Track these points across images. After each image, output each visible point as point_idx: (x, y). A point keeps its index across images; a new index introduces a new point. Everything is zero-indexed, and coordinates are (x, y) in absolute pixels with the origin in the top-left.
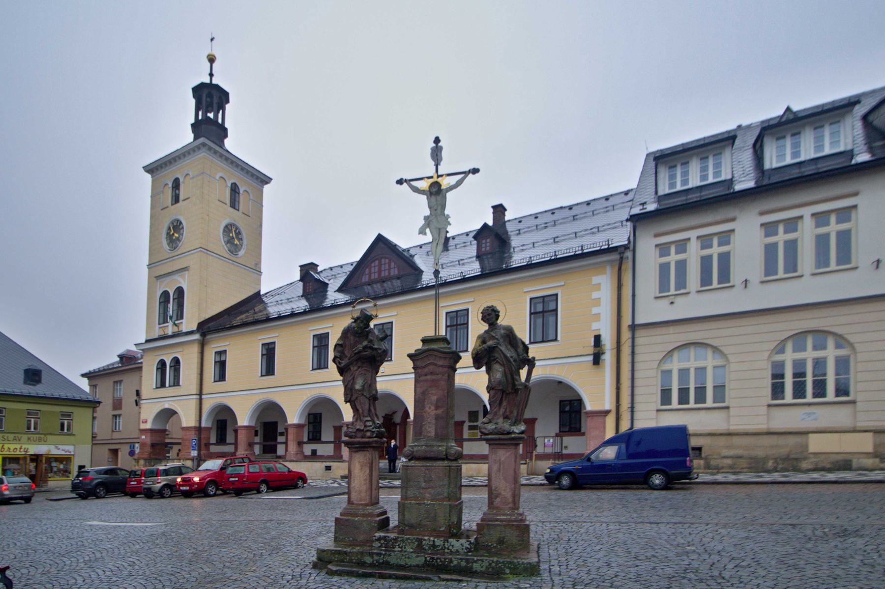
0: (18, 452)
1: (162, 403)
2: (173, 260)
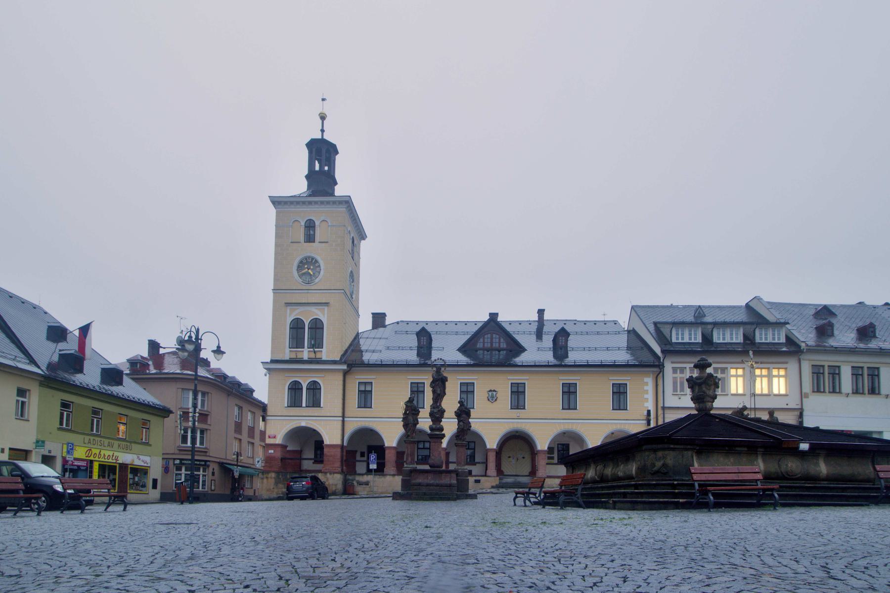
0: (110, 460)
1: (297, 422)
2: (308, 293)
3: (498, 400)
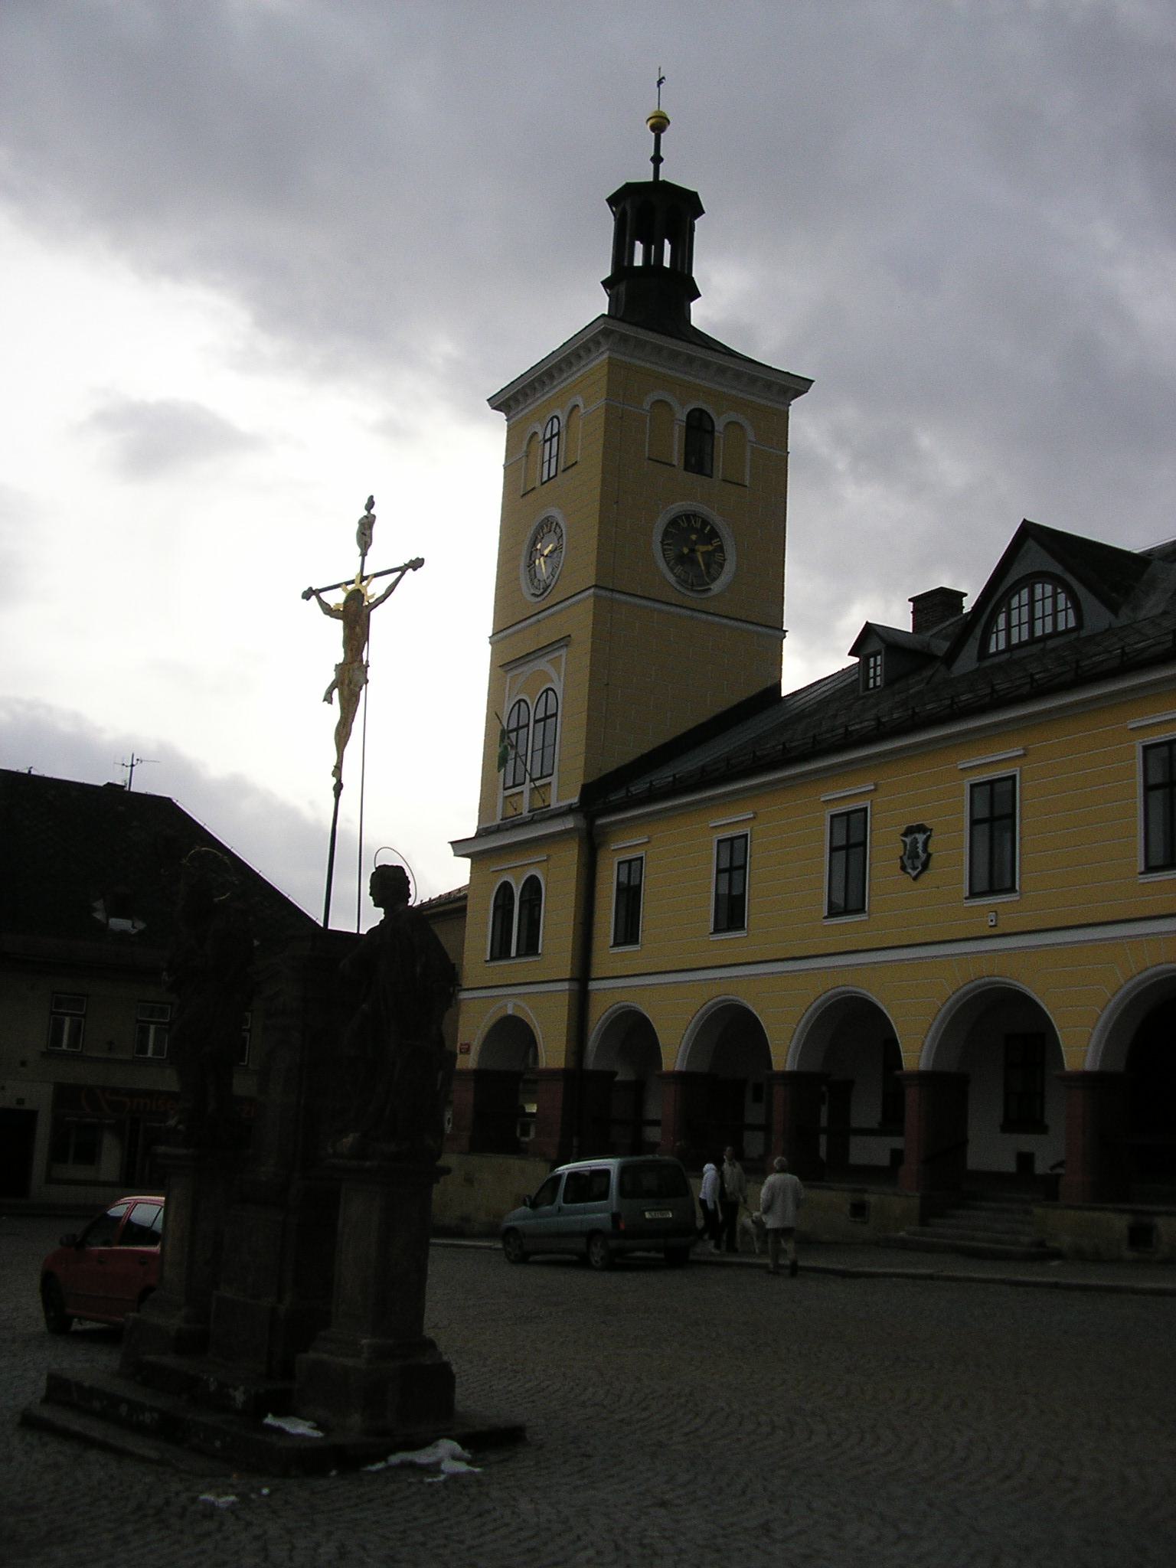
3: (932, 864)
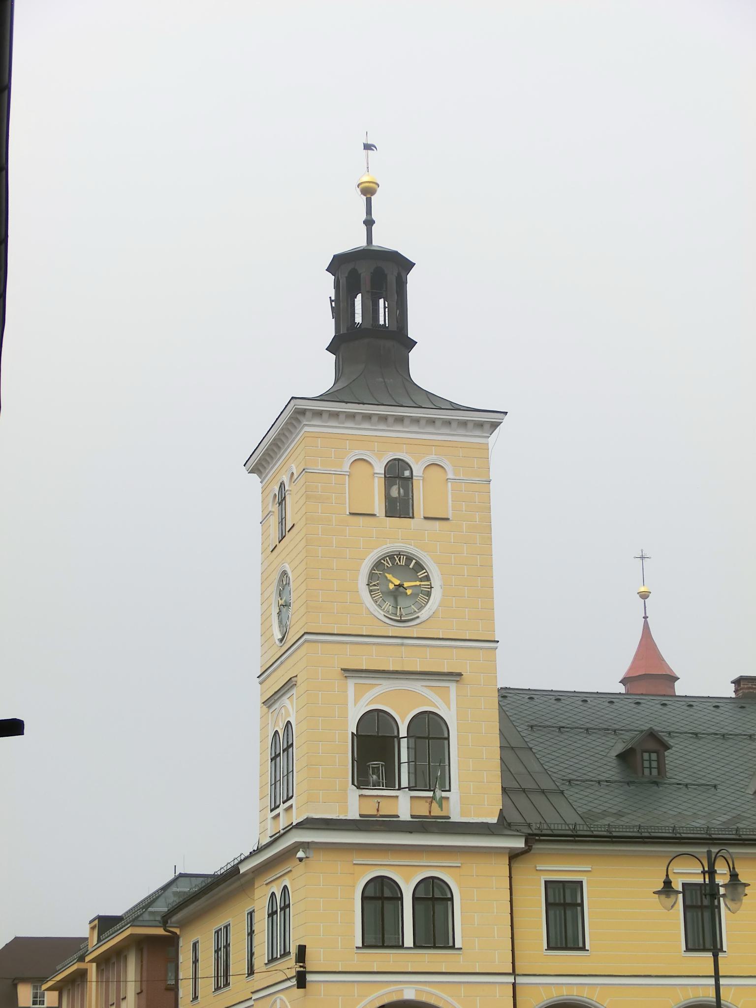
2: (402, 645)
